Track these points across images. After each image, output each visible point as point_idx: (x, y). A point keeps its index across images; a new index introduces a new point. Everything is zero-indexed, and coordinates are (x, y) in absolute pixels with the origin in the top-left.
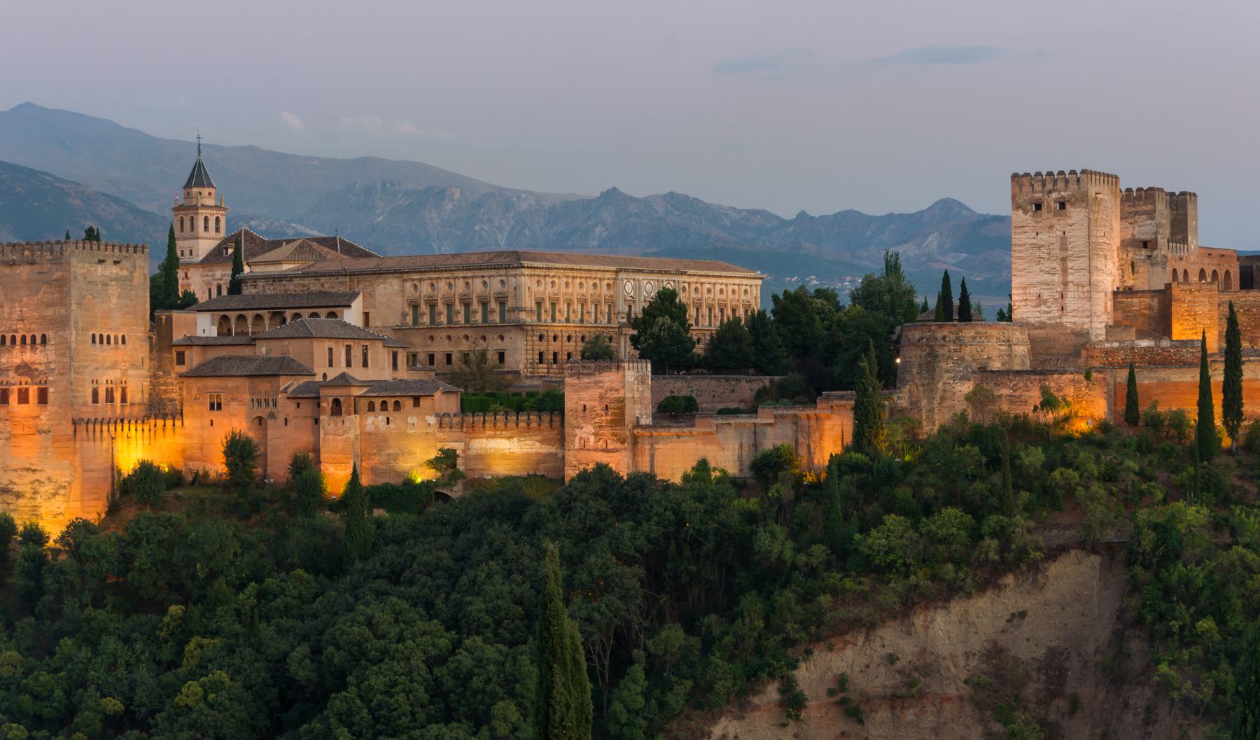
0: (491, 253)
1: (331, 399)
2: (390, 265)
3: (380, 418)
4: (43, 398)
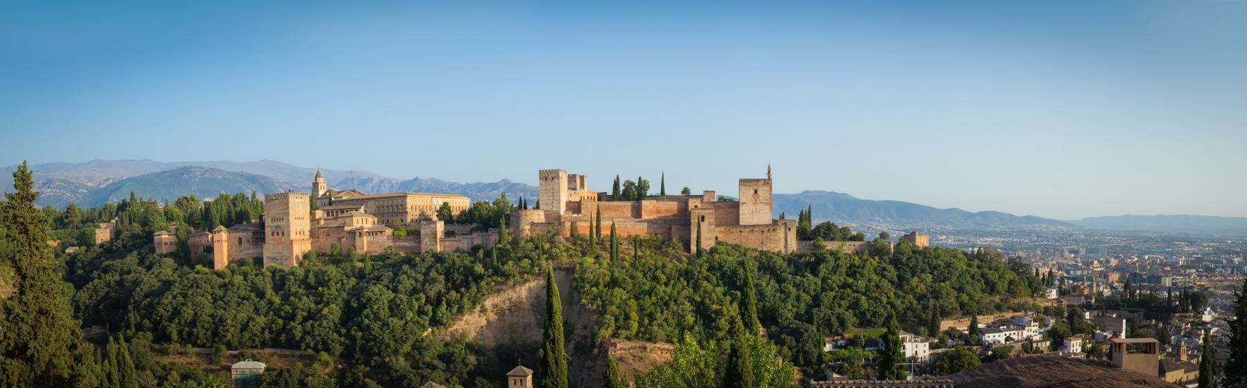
4: (283, 234)
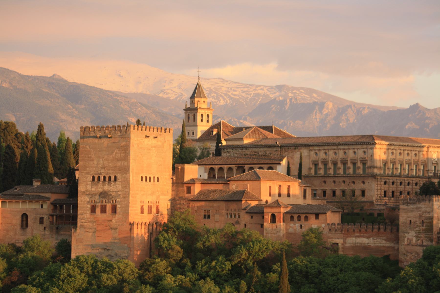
0: (358, 136)
1: (270, 215)
2: (303, 142)
3: (297, 225)
4: (114, 210)
